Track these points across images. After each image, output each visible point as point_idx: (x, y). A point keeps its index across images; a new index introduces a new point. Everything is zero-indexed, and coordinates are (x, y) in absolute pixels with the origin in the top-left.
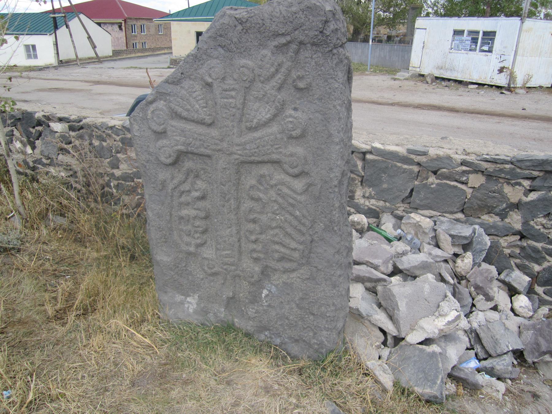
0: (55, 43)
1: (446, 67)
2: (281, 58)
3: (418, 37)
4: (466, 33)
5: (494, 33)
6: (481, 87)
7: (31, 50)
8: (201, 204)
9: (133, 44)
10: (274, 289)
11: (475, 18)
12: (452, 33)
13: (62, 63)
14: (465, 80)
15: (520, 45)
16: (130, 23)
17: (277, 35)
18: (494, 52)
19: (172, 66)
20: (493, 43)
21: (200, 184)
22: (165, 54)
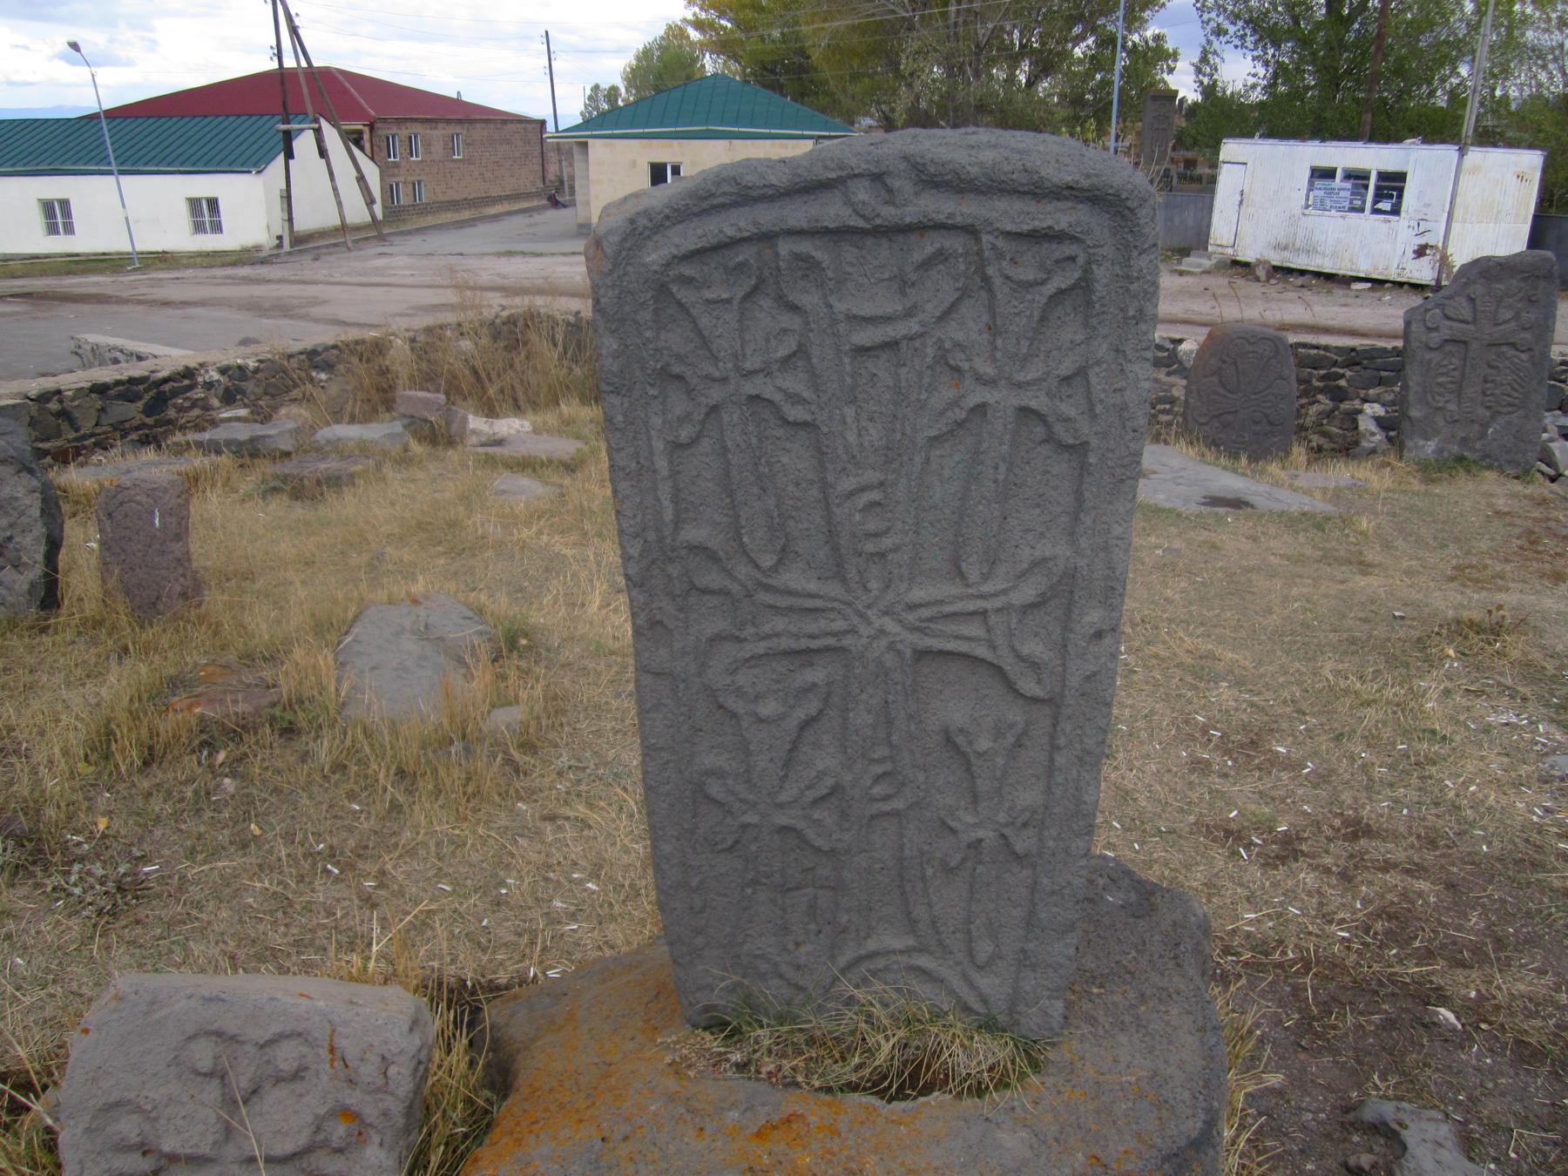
0: (285, 194)
1: (1297, 245)
2: (1523, 285)
3: (1228, 182)
5: (1401, 177)
6: (1376, 286)
7: (206, 213)
8: (1453, 373)
9: (392, 186)
10: (1498, 427)
11: (1360, 144)
12: (1308, 173)
13: (302, 242)
14: (1341, 272)
15: (1458, 200)
16: (383, 131)
17: (1523, 272)
18: (1403, 214)
20: (1400, 196)
21: (1455, 361)
22: (509, 213)
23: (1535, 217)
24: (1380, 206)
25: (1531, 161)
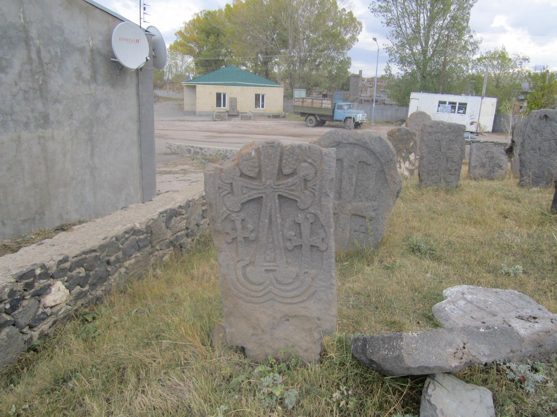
4: (447, 103)
5: (466, 104)
11: (453, 95)
15: (481, 110)
19: (217, 119)
20: (465, 109)
23: (495, 115)
24: (460, 111)
25: (494, 101)
